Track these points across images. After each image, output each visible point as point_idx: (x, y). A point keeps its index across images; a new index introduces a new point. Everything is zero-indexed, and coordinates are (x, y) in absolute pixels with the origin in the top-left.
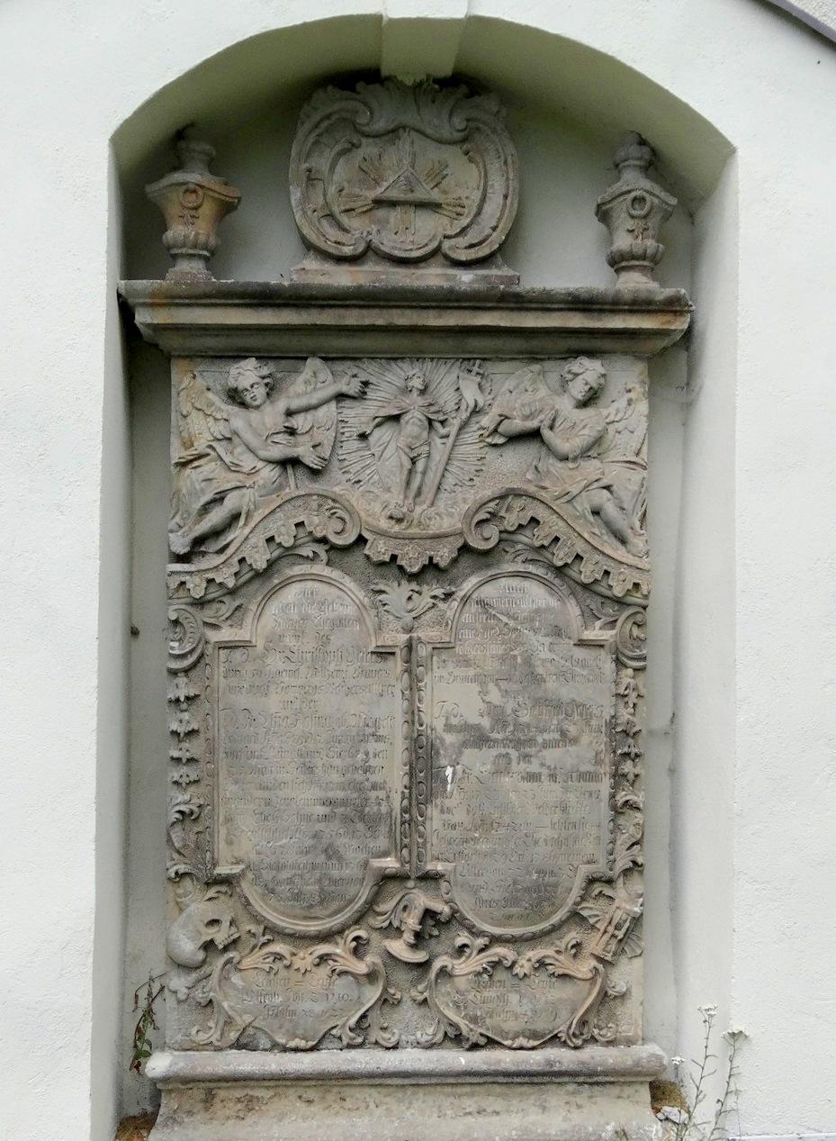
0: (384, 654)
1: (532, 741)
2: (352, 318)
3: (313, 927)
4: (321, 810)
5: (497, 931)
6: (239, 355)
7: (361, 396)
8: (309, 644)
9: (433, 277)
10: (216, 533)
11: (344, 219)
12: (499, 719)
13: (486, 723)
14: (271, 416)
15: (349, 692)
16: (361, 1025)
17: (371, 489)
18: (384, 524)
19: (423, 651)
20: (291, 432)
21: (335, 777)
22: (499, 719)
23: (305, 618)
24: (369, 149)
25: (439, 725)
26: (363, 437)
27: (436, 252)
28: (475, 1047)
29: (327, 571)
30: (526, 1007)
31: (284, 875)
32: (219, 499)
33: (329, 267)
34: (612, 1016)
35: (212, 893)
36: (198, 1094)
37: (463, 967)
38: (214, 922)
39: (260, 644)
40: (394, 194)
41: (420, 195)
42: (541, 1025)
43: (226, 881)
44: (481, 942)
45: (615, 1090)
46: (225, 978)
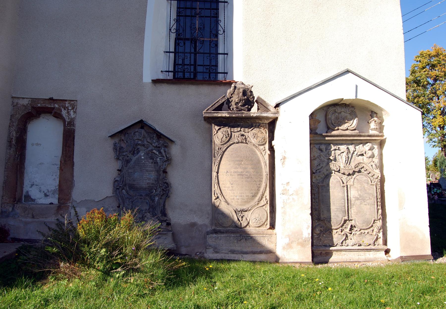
1: (365, 199)
5: (361, 228)
9: (347, 132)
12: (360, 196)
13: (359, 197)
16: (342, 243)
21: (338, 205)
22: (360, 196)
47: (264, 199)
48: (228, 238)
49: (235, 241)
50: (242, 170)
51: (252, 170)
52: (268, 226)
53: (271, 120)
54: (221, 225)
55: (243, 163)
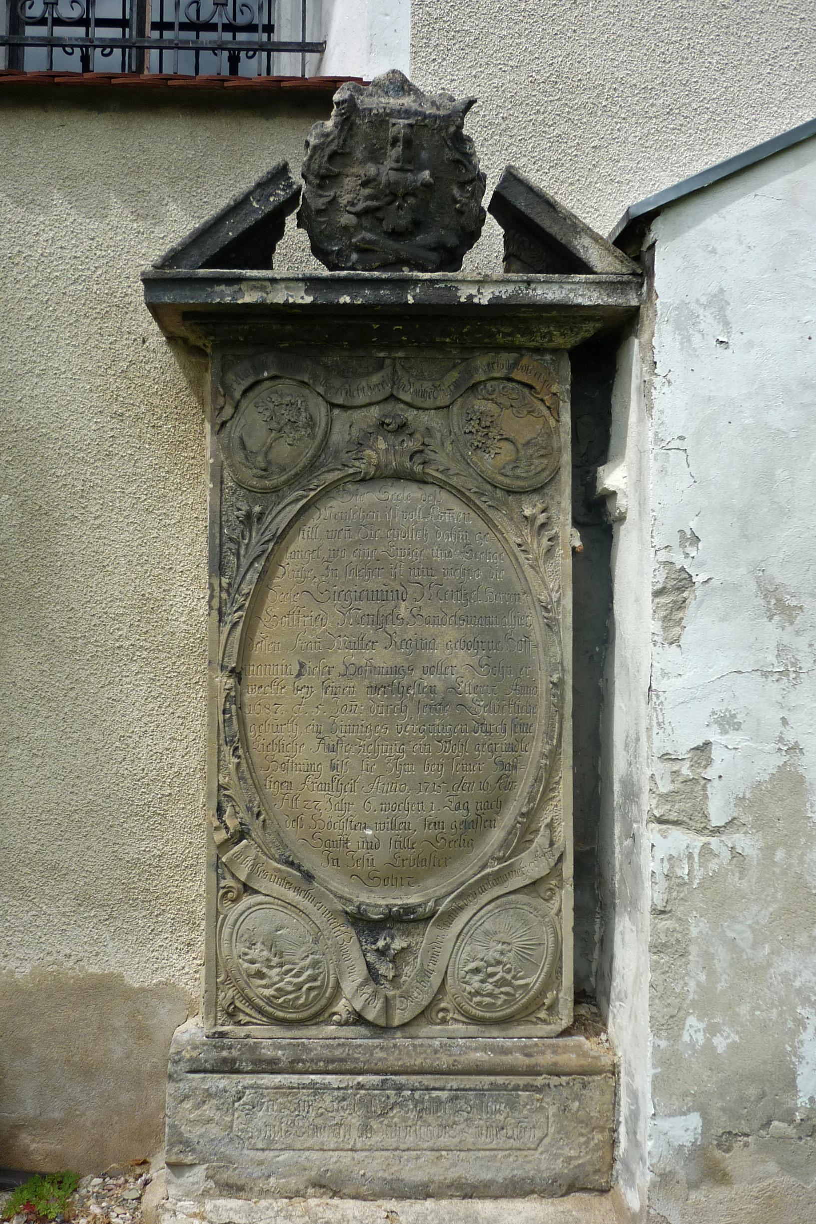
47: (541, 840)
48: (303, 1094)
49: (355, 1121)
50: (400, 661)
51: (461, 659)
52: (565, 1018)
53: (588, 330)
54: (260, 1011)
55: (403, 610)
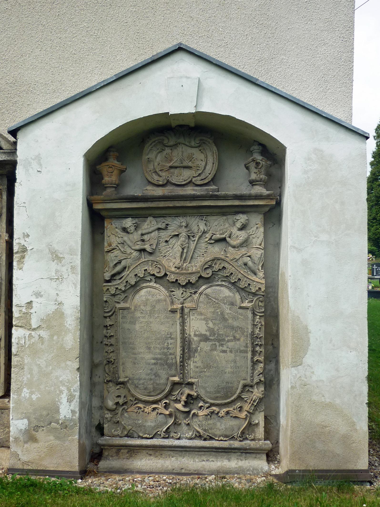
0: (173, 311)
2: (162, 204)
3: (151, 399)
4: (153, 361)
6: (126, 217)
7: (166, 228)
8: (148, 308)
9: (189, 191)
10: (119, 273)
11: (160, 173)
14: (136, 236)
15: (162, 324)
17: (170, 259)
18: (173, 269)
19: (186, 310)
20: (143, 241)
23: (147, 300)
24: (168, 151)
25: (192, 334)
26: (167, 241)
27: (191, 182)
28: (205, 440)
29: (155, 285)
30: (223, 427)
31: (141, 382)
32: (120, 262)
33: (155, 188)
34: (253, 431)
35: (118, 387)
36: (114, 450)
37: (201, 413)
38: (119, 396)
39: (133, 308)
40: (176, 164)
41: (185, 164)
42: (228, 433)
43: (123, 383)
44: (207, 405)
45: (254, 455)
46: (122, 414)
